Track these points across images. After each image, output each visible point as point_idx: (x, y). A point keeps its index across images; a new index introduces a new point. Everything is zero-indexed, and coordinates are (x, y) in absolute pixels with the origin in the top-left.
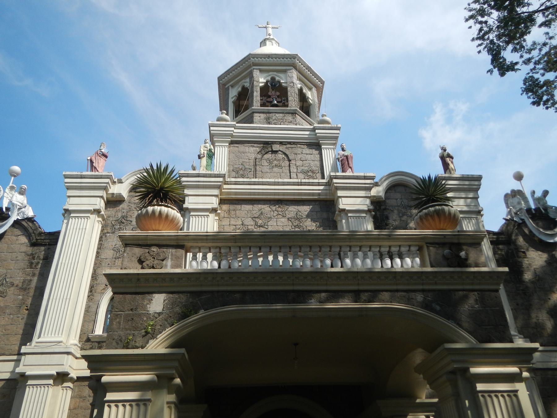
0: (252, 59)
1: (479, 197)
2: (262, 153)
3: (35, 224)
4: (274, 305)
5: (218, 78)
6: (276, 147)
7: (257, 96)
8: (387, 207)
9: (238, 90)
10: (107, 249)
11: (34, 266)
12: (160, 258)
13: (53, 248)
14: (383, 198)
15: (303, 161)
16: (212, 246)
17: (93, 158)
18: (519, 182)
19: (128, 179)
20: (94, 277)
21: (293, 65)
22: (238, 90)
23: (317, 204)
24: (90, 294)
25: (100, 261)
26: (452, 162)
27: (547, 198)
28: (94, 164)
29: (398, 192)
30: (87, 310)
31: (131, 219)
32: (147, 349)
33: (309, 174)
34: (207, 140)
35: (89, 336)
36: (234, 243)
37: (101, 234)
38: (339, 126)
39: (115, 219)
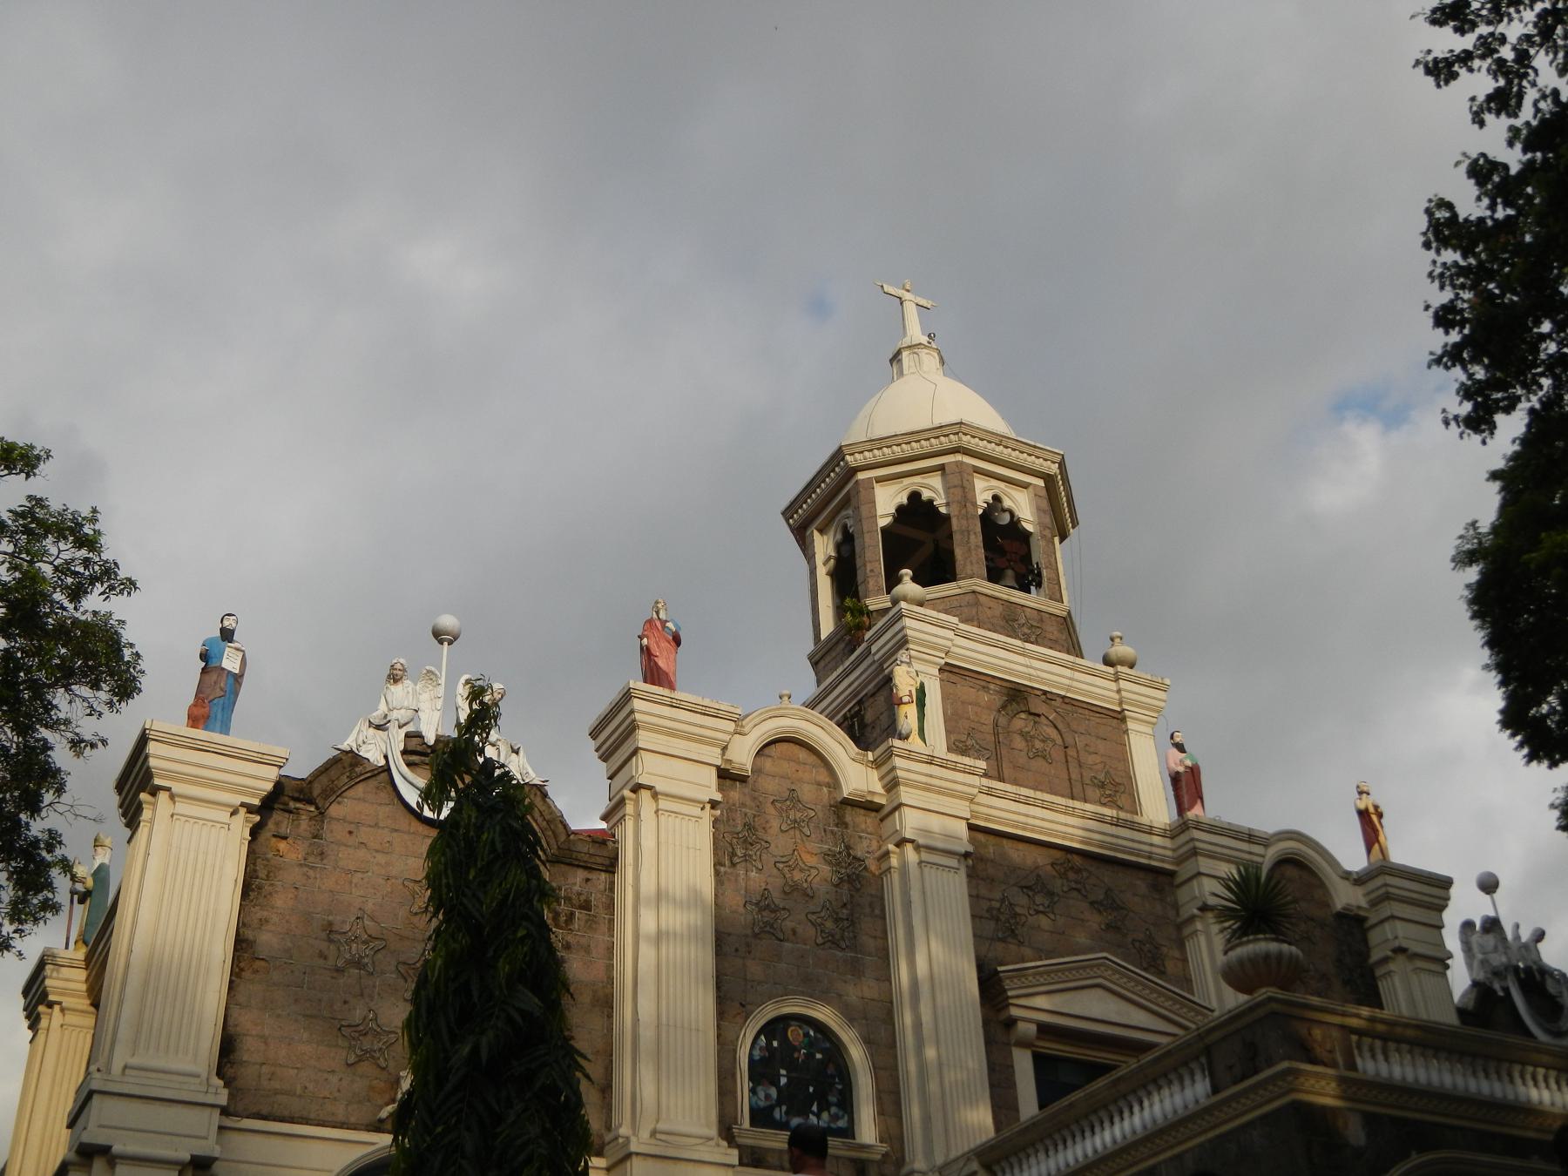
1: (1442, 927)
3: (549, 807)
6: (1037, 706)
11: (563, 919)
18: (1488, 896)
27: (1540, 946)
38: (1167, 681)
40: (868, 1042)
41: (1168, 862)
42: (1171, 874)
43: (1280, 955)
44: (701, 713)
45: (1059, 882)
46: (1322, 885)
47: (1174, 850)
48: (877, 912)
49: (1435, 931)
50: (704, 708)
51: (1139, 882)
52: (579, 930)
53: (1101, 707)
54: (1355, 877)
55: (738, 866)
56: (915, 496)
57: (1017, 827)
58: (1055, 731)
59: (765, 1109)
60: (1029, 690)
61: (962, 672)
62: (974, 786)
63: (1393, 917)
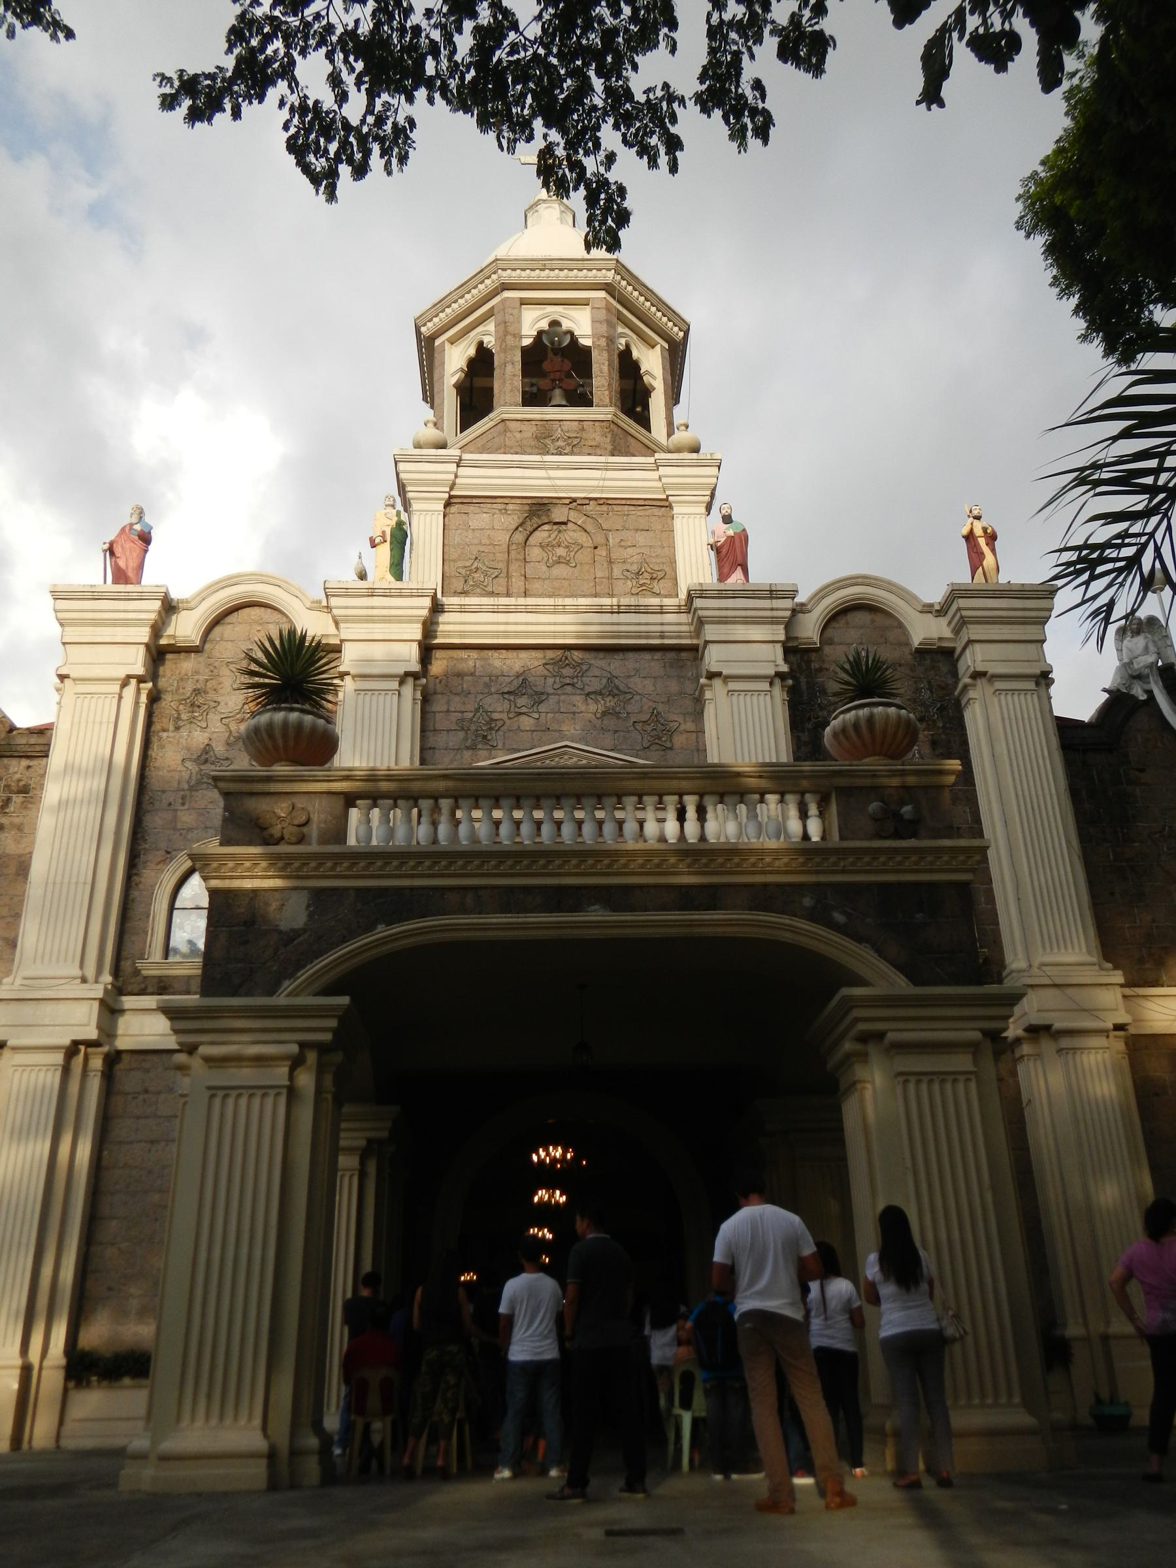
0: (500, 271)
1: (1043, 641)
2: (526, 530)
4: (521, 915)
6: (559, 514)
7: (514, 375)
8: (826, 666)
9: (466, 355)
12: (296, 822)
14: (815, 644)
19: (204, 599)
23: (655, 657)
26: (993, 551)
29: (853, 627)
31: (216, 699)
32: (279, 996)
35: (137, 965)
39: (177, 697)
41: (686, 638)
42: (694, 649)
43: (270, 725)
44: (125, 599)
45: (550, 681)
46: (901, 625)
47: (692, 624)
49: (1032, 647)
50: (127, 594)
51: (652, 664)
52: (14, 812)
53: (645, 499)
54: (937, 607)
55: (182, 730)
57: (498, 637)
58: (585, 534)
60: (555, 501)
61: (474, 501)
62: (422, 608)
63: (970, 642)
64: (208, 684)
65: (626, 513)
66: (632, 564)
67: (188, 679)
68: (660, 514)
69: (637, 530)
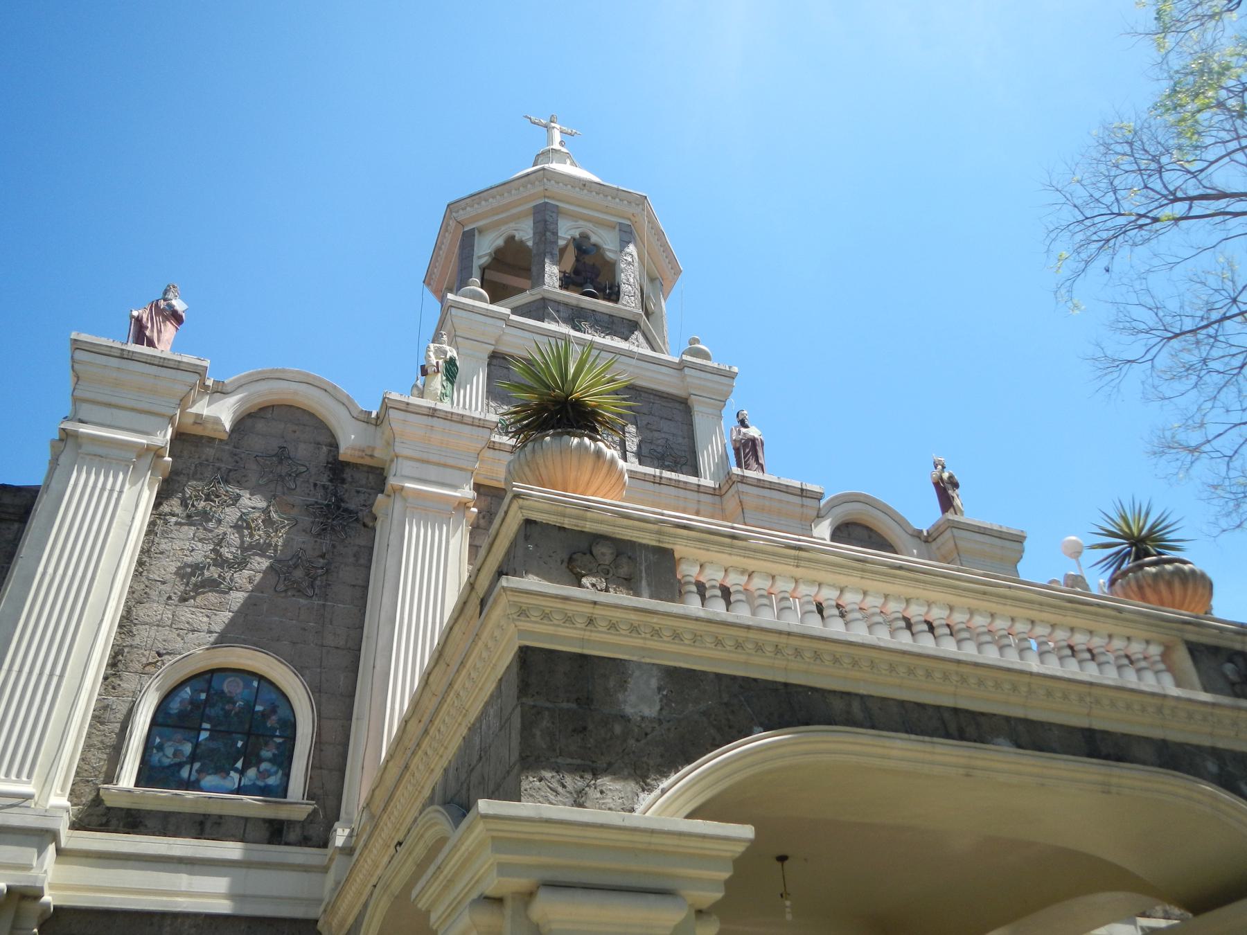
5: (448, 205)
10: (168, 557)
13: (9, 529)
15: (651, 430)
16: (731, 567)
17: (145, 317)
20: (124, 626)
21: (632, 218)
22: (492, 244)
24: (110, 672)
25: (147, 586)
28: (148, 333)
30: (99, 718)
33: (666, 463)
34: (444, 336)
36: (793, 565)
37: (153, 516)
38: (735, 369)
40: (317, 691)
48: (362, 561)
56: (510, 240)
59: (170, 766)
64: (231, 474)
65: (652, 401)
66: (658, 445)
67: (209, 465)
68: (681, 408)
69: (661, 418)
